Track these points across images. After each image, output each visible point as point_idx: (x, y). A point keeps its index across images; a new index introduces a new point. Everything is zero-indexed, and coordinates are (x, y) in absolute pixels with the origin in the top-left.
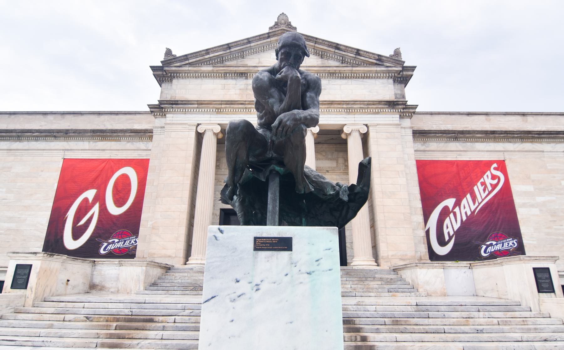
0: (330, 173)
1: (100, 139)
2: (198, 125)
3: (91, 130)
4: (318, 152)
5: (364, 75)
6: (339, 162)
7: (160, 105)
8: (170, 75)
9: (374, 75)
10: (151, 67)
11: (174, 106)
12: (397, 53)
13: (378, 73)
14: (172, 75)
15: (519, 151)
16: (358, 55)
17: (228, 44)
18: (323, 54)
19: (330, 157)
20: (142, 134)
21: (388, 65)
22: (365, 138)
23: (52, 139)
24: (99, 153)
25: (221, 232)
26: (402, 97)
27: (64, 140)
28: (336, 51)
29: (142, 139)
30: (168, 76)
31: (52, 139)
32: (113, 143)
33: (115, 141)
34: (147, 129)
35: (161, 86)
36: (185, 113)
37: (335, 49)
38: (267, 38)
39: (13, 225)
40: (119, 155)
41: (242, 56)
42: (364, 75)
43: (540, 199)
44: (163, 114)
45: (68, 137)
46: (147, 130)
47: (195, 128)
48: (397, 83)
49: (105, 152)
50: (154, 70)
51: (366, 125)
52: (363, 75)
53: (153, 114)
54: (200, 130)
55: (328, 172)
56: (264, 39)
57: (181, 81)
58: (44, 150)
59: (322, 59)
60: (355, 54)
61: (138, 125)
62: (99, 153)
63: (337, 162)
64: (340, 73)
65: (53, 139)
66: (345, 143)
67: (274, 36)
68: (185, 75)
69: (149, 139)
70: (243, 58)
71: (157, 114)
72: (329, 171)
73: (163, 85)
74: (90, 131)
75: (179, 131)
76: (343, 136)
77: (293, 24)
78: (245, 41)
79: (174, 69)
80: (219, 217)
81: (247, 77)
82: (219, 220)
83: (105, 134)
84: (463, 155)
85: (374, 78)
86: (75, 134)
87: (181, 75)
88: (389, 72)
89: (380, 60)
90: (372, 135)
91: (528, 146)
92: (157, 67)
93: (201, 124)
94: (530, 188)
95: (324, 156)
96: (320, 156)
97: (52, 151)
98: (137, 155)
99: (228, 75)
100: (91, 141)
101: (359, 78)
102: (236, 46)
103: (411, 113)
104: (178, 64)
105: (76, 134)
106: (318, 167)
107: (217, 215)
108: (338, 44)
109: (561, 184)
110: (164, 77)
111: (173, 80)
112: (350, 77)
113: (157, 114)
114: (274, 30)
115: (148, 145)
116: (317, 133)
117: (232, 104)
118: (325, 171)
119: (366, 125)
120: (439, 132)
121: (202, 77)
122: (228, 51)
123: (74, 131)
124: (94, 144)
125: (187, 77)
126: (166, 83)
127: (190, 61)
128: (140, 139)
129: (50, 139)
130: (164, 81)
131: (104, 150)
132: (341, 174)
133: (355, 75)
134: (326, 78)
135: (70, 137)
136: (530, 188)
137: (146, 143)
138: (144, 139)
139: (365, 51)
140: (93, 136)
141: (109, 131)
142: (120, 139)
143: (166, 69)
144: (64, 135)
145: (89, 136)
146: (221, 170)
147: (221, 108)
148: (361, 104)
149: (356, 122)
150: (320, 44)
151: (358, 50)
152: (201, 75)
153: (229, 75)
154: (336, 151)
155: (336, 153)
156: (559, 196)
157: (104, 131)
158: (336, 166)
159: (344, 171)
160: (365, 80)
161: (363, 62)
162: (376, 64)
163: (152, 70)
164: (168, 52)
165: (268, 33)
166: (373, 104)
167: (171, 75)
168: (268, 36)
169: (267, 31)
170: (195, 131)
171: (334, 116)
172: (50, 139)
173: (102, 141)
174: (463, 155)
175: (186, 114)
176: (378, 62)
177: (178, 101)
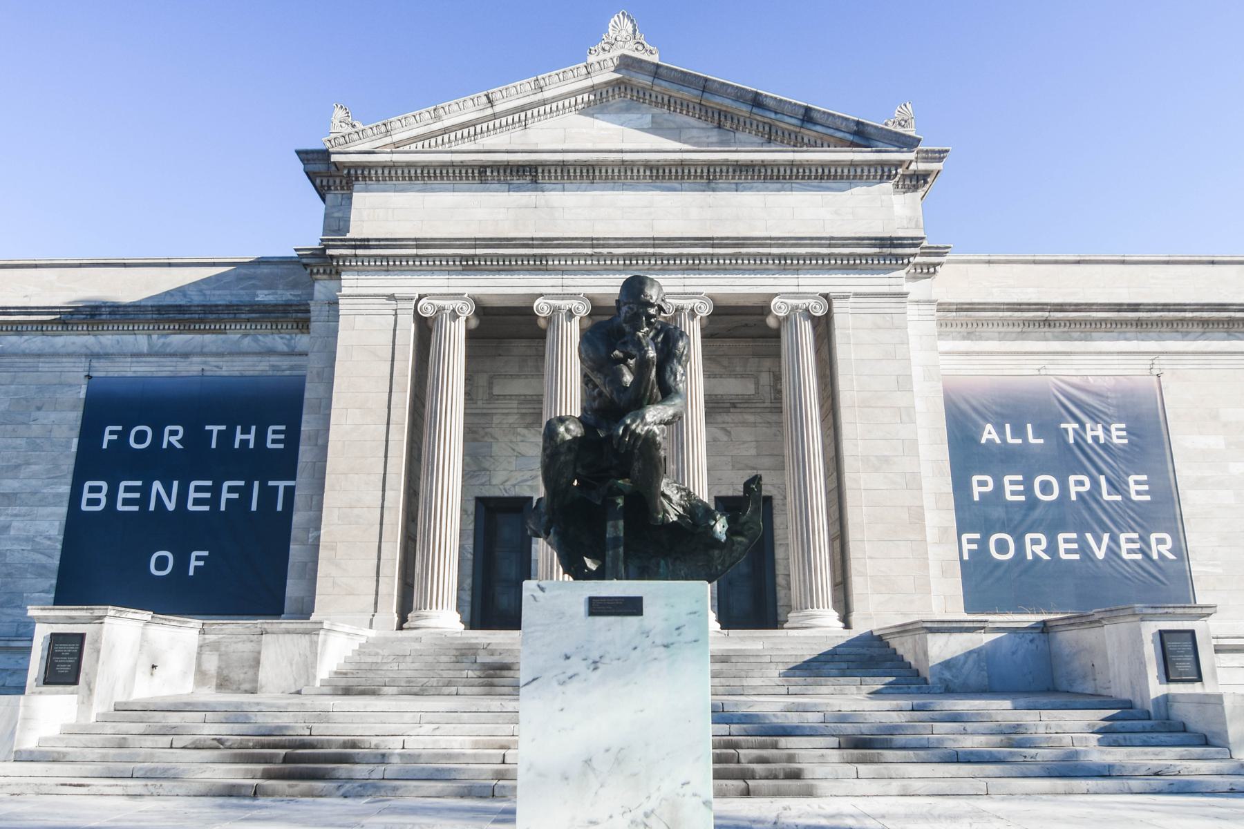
0: (739, 410)
1: (177, 327)
2: (421, 297)
3: (152, 306)
4: (710, 359)
5: (823, 170)
6: (761, 382)
7: (324, 250)
8: (346, 172)
9: (846, 171)
10: (298, 153)
13: (857, 165)
14: (352, 172)
16: (808, 122)
18: (722, 119)
19: (739, 369)
20: (279, 315)
22: (823, 327)
23: (57, 330)
24: (174, 364)
25: (542, 589)
26: (914, 226)
27: (88, 330)
29: (279, 327)
30: (340, 174)
31: (57, 330)
32: (208, 338)
33: (213, 333)
34: (290, 303)
35: (324, 200)
36: (386, 268)
37: (753, 106)
38: (585, 77)
40: (224, 368)
41: (524, 123)
42: (823, 170)
44: (334, 272)
45: (98, 324)
46: (291, 305)
48: (904, 190)
49: (189, 360)
50: (308, 160)
52: (820, 171)
53: (309, 271)
55: (735, 407)
59: (721, 130)
60: (801, 117)
61: (266, 292)
62: (174, 364)
63: (757, 384)
64: (764, 166)
65: (60, 328)
66: (775, 335)
68: (383, 172)
69: (295, 326)
71: (318, 271)
72: (738, 405)
73: (329, 197)
74: (150, 309)
75: (374, 312)
76: (771, 322)
80: (472, 517)
81: (535, 176)
82: (473, 524)
83: (187, 316)
84: (1060, 362)
85: (848, 177)
86: (113, 317)
87: (373, 172)
92: (313, 152)
93: (426, 295)
94: (1215, 442)
95: (725, 367)
96: (717, 369)
97: (60, 360)
98: (267, 368)
99: (489, 173)
100: (154, 334)
101: (809, 178)
103: (935, 265)
105: (118, 317)
106: (710, 395)
107: (469, 512)
110: (331, 176)
111: (355, 186)
112: (788, 177)
113: (318, 271)
115: (293, 341)
116: (708, 316)
118: (728, 405)
119: (826, 296)
120: (1005, 307)
121: (426, 179)
123: (111, 309)
124: (162, 340)
125: (387, 179)
126: (336, 192)
128: (274, 327)
129: (52, 330)
130: (332, 188)
131: (186, 355)
132: (768, 410)
133: (801, 170)
134: (730, 178)
135: (103, 322)
136: (1215, 442)
137: (288, 337)
138: (285, 327)
140: (157, 321)
141: (196, 309)
142: (225, 329)
144: (84, 319)
145: (148, 322)
146: (476, 403)
147: (473, 257)
148: (812, 246)
149: (802, 289)
150: (714, 93)
151: (808, 110)
152: (422, 171)
153: (492, 172)
154: (755, 355)
155: (757, 359)
157: (186, 308)
158: (754, 393)
159: (773, 405)
160: (824, 183)
161: (821, 139)
162: (852, 144)
163: (302, 160)
166: (843, 246)
167: (349, 172)
172: (52, 330)
173: (180, 334)
174: (1060, 362)
175: (388, 271)
177: (368, 240)
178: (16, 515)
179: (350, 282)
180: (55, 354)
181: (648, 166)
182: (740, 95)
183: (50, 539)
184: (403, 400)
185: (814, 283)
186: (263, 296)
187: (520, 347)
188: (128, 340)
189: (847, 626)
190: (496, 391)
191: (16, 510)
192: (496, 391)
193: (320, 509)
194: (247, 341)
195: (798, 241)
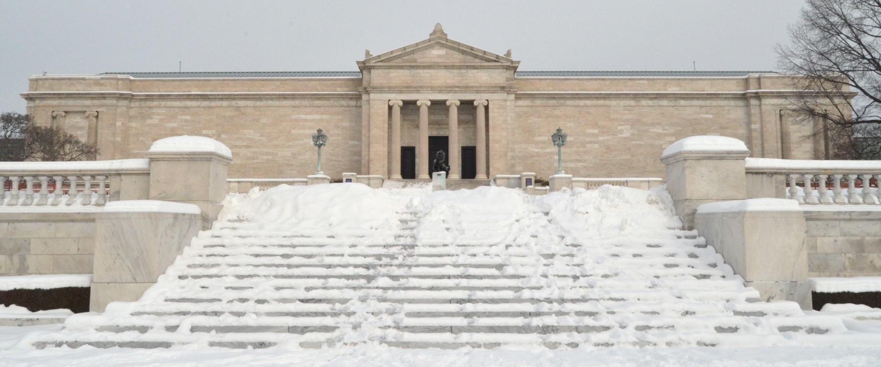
2: (390, 100)
10: (357, 62)
11: (375, 89)
12: (509, 54)
15: (594, 106)
17: (404, 48)
21: (503, 61)
22: (487, 108)
28: (472, 51)
32: (325, 102)
39: (270, 157)
43: (601, 138)
47: (387, 102)
51: (487, 100)
54: (391, 103)
56: (427, 43)
58: (279, 107)
66: (475, 108)
67: (433, 40)
70: (414, 54)
78: (415, 45)
79: (372, 64)
88: (503, 66)
89: (497, 59)
90: (490, 106)
91: (601, 102)
102: (409, 48)
104: (374, 61)
108: (472, 47)
109: (617, 128)
114: (432, 37)
117: (408, 88)
119: (487, 100)
122: (404, 52)
127: (382, 59)
131: (319, 107)
136: (596, 131)
139: (489, 53)
143: (367, 64)
147: (402, 91)
151: (485, 52)
156: (614, 136)
160: (489, 70)
162: (495, 61)
164: (368, 53)
165: (429, 39)
168: (430, 40)
169: (427, 37)
170: (387, 104)
171: (468, 94)
176: (497, 60)
178: (279, 151)
179: (372, 95)
180: (283, 107)
181: (445, 66)
182: (468, 47)
183: (288, 157)
187: (411, 107)
188: (303, 102)
191: (279, 149)
195: (481, 87)
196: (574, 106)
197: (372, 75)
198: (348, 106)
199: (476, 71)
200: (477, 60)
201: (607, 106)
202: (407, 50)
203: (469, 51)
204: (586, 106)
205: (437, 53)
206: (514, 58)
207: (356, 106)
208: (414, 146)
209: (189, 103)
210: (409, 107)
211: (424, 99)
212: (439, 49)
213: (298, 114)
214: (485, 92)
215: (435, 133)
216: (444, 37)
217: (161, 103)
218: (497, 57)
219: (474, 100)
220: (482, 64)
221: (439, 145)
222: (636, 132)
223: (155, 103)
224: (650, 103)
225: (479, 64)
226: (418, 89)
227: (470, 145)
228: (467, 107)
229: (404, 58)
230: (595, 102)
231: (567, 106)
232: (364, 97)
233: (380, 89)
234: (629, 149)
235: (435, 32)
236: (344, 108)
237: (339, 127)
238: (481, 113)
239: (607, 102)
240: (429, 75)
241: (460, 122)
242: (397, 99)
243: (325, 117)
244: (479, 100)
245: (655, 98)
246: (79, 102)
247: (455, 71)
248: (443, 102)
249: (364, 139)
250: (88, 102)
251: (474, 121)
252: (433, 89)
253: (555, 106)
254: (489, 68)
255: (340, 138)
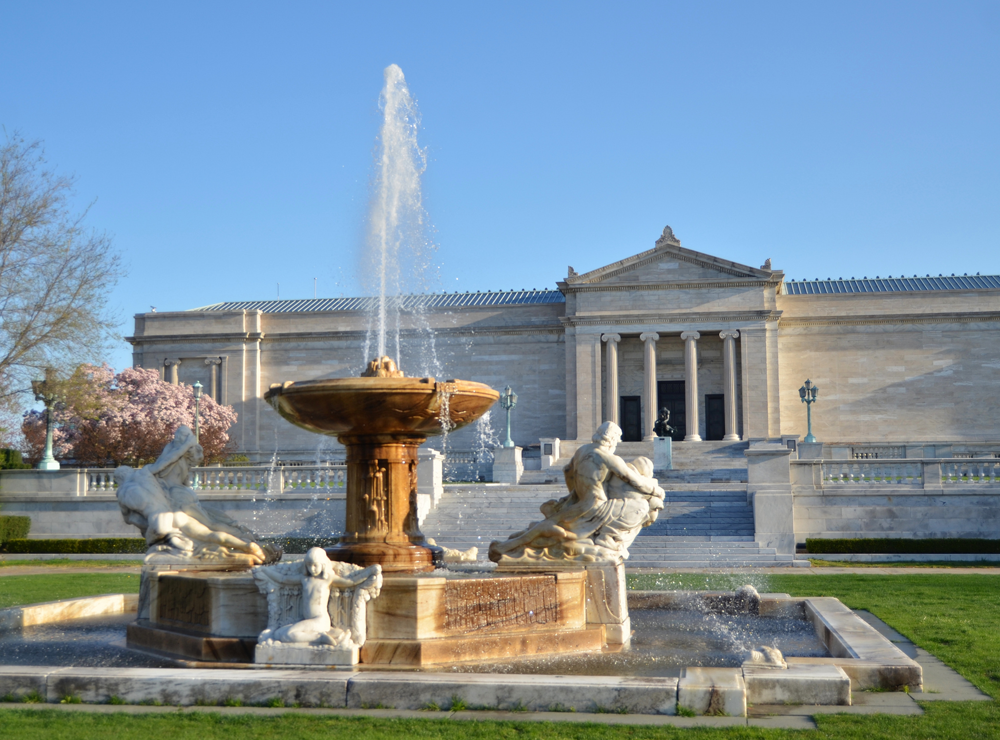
22: (738, 341)
32: (515, 337)
51: (738, 331)
54: (604, 339)
57: (584, 294)
77: (677, 237)
90: (745, 339)
91: (908, 326)
131: (508, 344)
136: (901, 369)
151: (733, 263)
162: (749, 276)
164: (571, 269)
168: (656, 250)
169: (654, 246)
182: (709, 257)
184: (599, 369)
185: (735, 325)
186: (534, 319)
187: (633, 340)
188: (486, 338)
189: (741, 438)
190: (626, 357)
192: (626, 357)
193: (576, 405)
194: (530, 337)
196: (867, 333)
197: (578, 300)
198: (548, 342)
199: (722, 290)
200: (723, 275)
201: (917, 331)
202: (625, 265)
203: (711, 262)
204: (885, 332)
205: (666, 265)
206: (774, 267)
207: (558, 342)
208: (638, 395)
209: (335, 343)
210: (630, 341)
211: (649, 332)
212: (670, 261)
213: (480, 354)
214: (734, 318)
215: (668, 377)
216: (676, 244)
217: (300, 343)
218: (751, 269)
219: (720, 331)
220: (730, 281)
221: (672, 394)
222: (961, 369)
223: (293, 344)
224: (983, 325)
225: (726, 281)
226: (640, 319)
227: (717, 392)
228: (709, 339)
229: (621, 275)
230: (899, 326)
231: (858, 333)
232: (568, 330)
233: (590, 321)
234: (952, 394)
235: (663, 239)
236: (542, 345)
237: (534, 371)
238: (731, 347)
239: (918, 326)
240: (656, 297)
241: (701, 362)
242: (613, 332)
243: (514, 357)
244: (727, 332)
245: (990, 318)
246: (197, 345)
247: (691, 291)
248: (678, 335)
249: (568, 387)
250: (208, 346)
251: (721, 361)
252: (661, 317)
253: (841, 334)
254: (740, 285)
255: (536, 386)
